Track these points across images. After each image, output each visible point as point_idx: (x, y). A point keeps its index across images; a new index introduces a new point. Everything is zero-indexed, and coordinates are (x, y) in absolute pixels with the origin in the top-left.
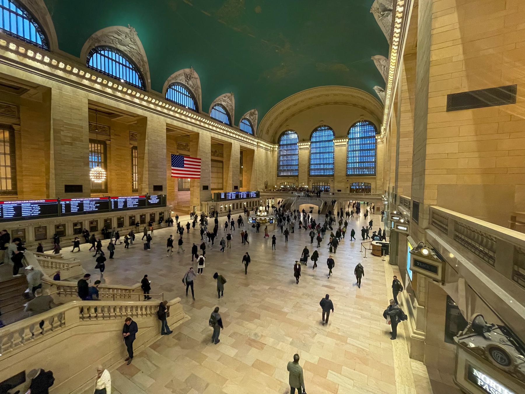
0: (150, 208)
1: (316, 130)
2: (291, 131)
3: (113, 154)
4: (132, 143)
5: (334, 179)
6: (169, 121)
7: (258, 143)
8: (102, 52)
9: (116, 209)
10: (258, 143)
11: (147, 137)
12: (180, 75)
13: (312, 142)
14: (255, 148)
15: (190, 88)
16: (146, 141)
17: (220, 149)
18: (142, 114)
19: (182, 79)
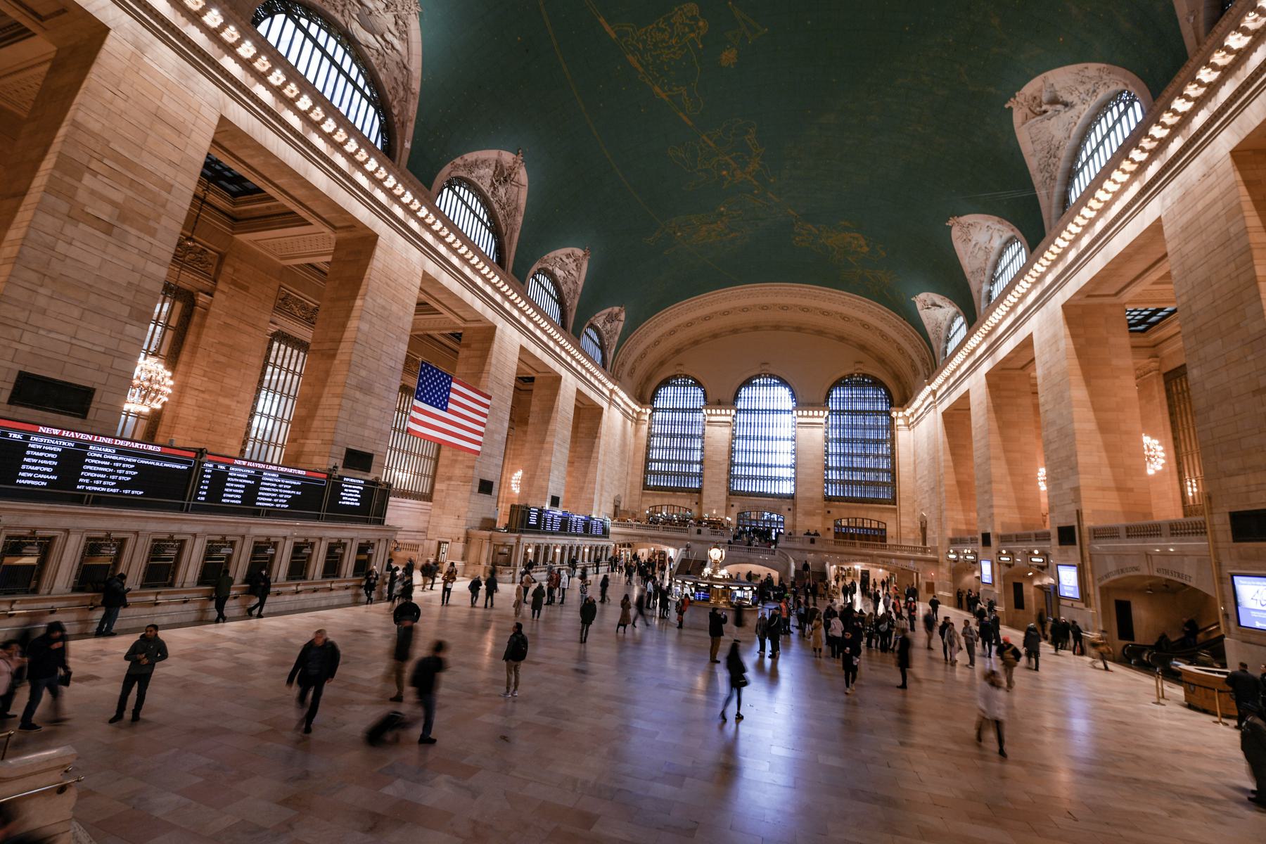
0: (333, 519)
1: (748, 383)
2: (687, 377)
3: (209, 336)
4: (278, 321)
5: (795, 505)
6: (432, 268)
7: (612, 391)
8: (304, 22)
9: (214, 505)
10: (612, 391)
11: (361, 292)
12: (486, 160)
13: (738, 411)
14: (605, 405)
15: (496, 206)
16: (358, 302)
17: (533, 386)
18: (367, 223)
19: (484, 177)
